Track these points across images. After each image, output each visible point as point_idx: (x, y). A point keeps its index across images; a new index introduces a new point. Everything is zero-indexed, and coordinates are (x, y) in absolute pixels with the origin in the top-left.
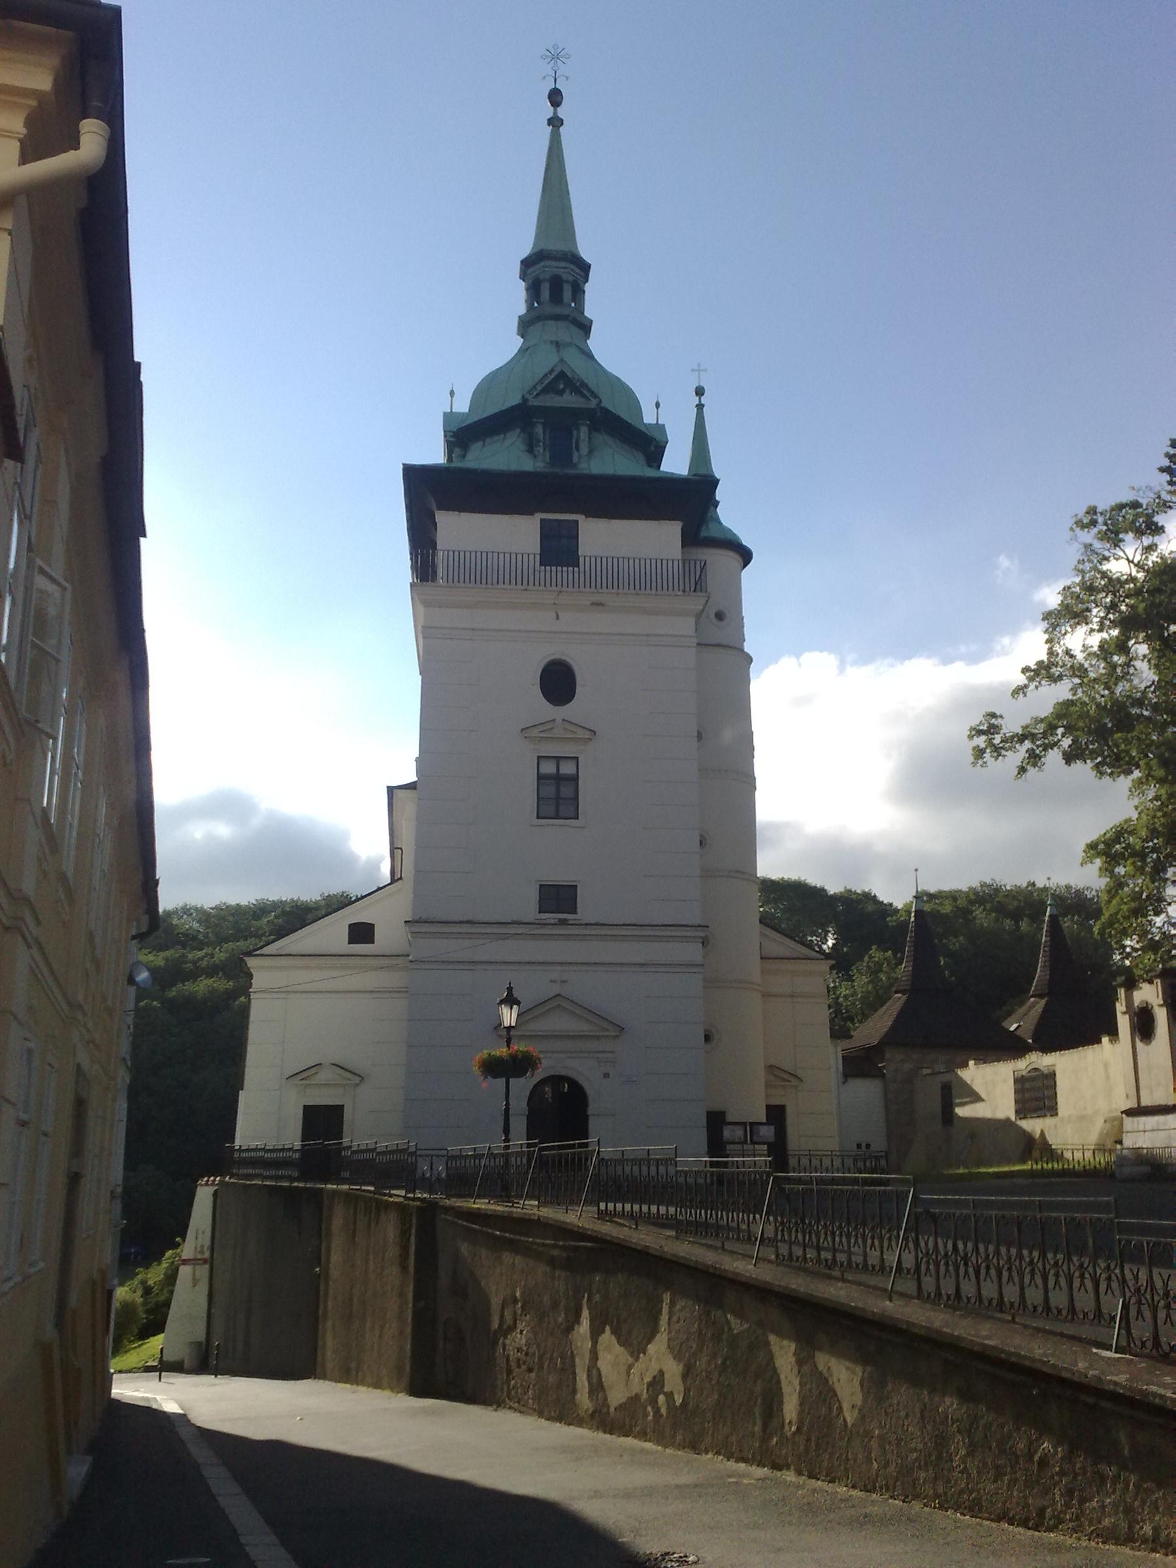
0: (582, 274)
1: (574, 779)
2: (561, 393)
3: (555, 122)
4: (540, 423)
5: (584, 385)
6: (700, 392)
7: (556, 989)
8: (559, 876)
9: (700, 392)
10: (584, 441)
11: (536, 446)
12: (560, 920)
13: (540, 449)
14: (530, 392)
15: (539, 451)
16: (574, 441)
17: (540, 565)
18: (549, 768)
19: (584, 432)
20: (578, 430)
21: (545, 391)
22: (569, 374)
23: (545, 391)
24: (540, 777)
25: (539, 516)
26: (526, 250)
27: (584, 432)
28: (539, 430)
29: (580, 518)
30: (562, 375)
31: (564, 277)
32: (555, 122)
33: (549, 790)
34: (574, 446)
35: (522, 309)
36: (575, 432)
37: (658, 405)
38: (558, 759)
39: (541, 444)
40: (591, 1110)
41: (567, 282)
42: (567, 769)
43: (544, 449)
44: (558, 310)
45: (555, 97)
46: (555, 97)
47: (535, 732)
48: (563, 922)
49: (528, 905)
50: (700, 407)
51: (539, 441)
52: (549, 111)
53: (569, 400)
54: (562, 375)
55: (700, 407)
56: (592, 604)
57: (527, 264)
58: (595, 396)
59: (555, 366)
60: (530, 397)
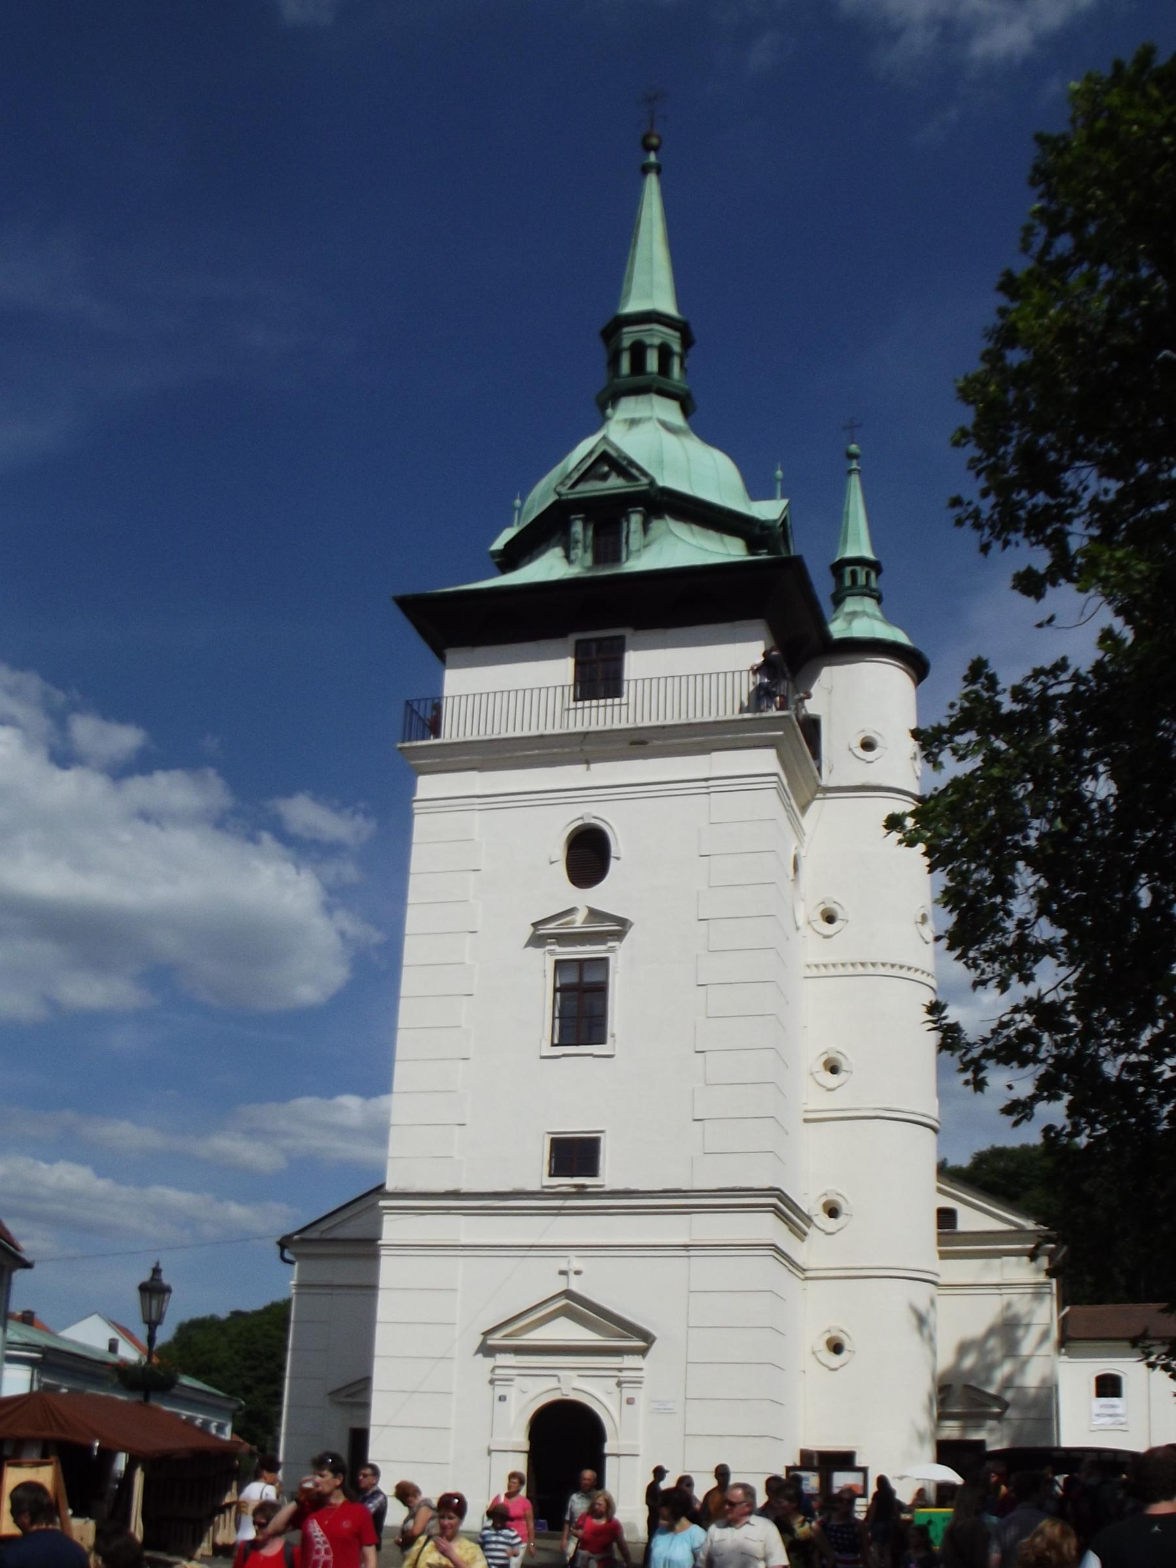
0: (677, 334)
1: (601, 989)
2: (604, 477)
4: (578, 519)
5: (632, 463)
7: (560, 1285)
8: (574, 1125)
10: (635, 532)
11: (574, 549)
12: (576, 1186)
13: (578, 552)
14: (562, 483)
15: (576, 554)
16: (624, 534)
17: (576, 700)
18: (571, 978)
19: (636, 520)
20: (628, 521)
21: (582, 478)
22: (613, 453)
23: (582, 478)
25: (573, 638)
27: (636, 520)
31: (648, 341)
34: (624, 540)
36: (625, 524)
38: (581, 963)
39: (580, 545)
40: (608, 1448)
41: (651, 346)
42: (591, 977)
43: (585, 551)
44: (640, 380)
47: (550, 928)
48: (581, 1192)
51: (577, 542)
53: (615, 483)
56: (633, 743)
58: (644, 473)
59: (596, 446)
60: (564, 490)
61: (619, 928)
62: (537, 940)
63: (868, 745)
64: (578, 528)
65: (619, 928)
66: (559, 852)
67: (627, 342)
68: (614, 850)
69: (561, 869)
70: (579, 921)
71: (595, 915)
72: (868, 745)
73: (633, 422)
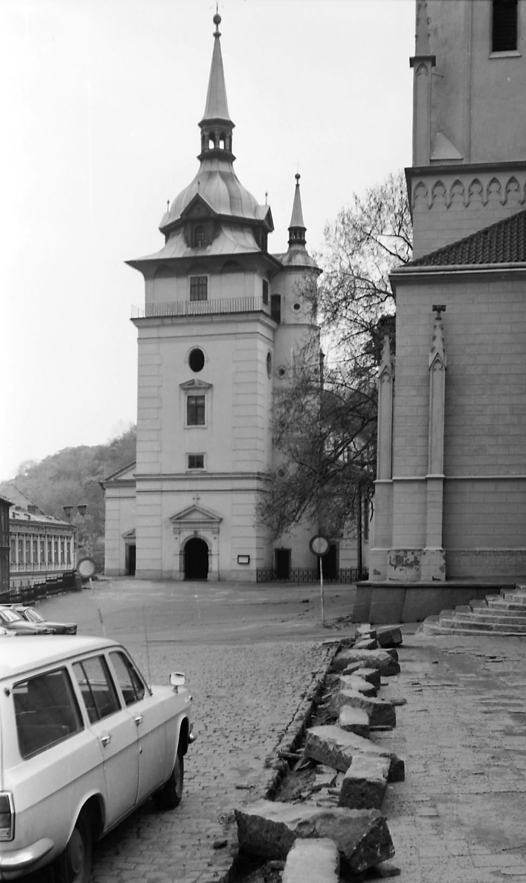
1: (203, 406)
3: (217, 35)
6: (298, 177)
8: (196, 451)
9: (298, 177)
18: (193, 402)
24: (189, 406)
25: (189, 276)
26: (200, 118)
29: (208, 275)
32: (217, 35)
35: (199, 153)
37: (266, 195)
38: (197, 398)
42: (200, 402)
45: (217, 20)
46: (217, 20)
50: (298, 186)
52: (213, 28)
55: (298, 186)
57: (201, 125)
68: (205, 359)
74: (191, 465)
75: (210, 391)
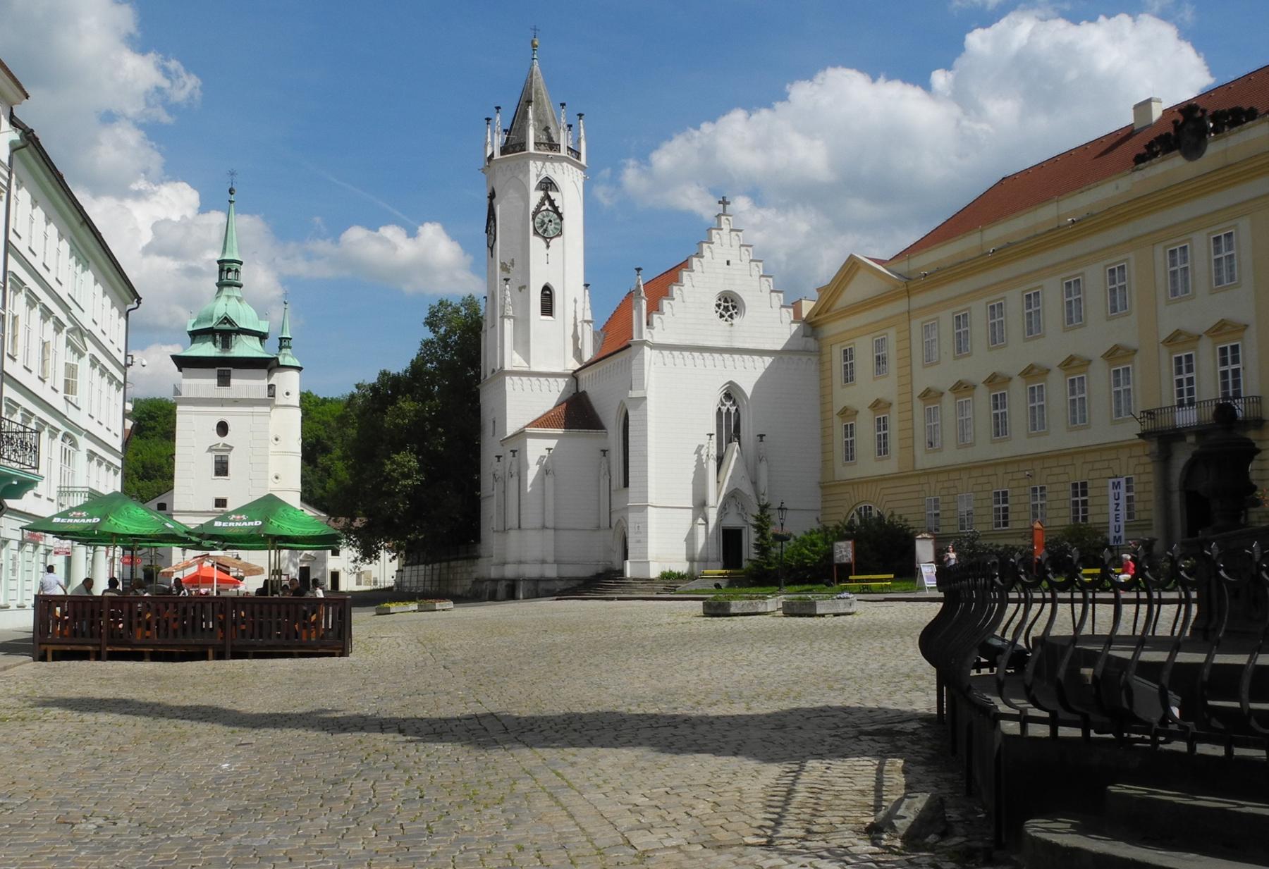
1: (227, 463)
2: (225, 324)
13: (218, 344)
19: (233, 336)
24: (216, 462)
25: (217, 368)
28: (218, 337)
30: (226, 318)
33: (219, 466)
35: (217, 281)
45: (231, 191)
46: (231, 191)
47: (214, 447)
49: (211, 506)
53: (228, 326)
54: (226, 318)
61: (231, 448)
62: (210, 450)
63: (288, 394)
64: (218, 337)
65: (231, 448)
66: (215, 428)
67: (226, 268)
69: (215, 432)
70: (220, 447)
71: (225, 445)
72: (288, 394)
73: (229, 297)
74: (217, 506)
75: (232, 453)
